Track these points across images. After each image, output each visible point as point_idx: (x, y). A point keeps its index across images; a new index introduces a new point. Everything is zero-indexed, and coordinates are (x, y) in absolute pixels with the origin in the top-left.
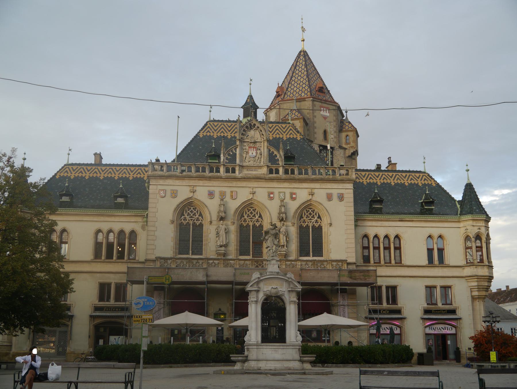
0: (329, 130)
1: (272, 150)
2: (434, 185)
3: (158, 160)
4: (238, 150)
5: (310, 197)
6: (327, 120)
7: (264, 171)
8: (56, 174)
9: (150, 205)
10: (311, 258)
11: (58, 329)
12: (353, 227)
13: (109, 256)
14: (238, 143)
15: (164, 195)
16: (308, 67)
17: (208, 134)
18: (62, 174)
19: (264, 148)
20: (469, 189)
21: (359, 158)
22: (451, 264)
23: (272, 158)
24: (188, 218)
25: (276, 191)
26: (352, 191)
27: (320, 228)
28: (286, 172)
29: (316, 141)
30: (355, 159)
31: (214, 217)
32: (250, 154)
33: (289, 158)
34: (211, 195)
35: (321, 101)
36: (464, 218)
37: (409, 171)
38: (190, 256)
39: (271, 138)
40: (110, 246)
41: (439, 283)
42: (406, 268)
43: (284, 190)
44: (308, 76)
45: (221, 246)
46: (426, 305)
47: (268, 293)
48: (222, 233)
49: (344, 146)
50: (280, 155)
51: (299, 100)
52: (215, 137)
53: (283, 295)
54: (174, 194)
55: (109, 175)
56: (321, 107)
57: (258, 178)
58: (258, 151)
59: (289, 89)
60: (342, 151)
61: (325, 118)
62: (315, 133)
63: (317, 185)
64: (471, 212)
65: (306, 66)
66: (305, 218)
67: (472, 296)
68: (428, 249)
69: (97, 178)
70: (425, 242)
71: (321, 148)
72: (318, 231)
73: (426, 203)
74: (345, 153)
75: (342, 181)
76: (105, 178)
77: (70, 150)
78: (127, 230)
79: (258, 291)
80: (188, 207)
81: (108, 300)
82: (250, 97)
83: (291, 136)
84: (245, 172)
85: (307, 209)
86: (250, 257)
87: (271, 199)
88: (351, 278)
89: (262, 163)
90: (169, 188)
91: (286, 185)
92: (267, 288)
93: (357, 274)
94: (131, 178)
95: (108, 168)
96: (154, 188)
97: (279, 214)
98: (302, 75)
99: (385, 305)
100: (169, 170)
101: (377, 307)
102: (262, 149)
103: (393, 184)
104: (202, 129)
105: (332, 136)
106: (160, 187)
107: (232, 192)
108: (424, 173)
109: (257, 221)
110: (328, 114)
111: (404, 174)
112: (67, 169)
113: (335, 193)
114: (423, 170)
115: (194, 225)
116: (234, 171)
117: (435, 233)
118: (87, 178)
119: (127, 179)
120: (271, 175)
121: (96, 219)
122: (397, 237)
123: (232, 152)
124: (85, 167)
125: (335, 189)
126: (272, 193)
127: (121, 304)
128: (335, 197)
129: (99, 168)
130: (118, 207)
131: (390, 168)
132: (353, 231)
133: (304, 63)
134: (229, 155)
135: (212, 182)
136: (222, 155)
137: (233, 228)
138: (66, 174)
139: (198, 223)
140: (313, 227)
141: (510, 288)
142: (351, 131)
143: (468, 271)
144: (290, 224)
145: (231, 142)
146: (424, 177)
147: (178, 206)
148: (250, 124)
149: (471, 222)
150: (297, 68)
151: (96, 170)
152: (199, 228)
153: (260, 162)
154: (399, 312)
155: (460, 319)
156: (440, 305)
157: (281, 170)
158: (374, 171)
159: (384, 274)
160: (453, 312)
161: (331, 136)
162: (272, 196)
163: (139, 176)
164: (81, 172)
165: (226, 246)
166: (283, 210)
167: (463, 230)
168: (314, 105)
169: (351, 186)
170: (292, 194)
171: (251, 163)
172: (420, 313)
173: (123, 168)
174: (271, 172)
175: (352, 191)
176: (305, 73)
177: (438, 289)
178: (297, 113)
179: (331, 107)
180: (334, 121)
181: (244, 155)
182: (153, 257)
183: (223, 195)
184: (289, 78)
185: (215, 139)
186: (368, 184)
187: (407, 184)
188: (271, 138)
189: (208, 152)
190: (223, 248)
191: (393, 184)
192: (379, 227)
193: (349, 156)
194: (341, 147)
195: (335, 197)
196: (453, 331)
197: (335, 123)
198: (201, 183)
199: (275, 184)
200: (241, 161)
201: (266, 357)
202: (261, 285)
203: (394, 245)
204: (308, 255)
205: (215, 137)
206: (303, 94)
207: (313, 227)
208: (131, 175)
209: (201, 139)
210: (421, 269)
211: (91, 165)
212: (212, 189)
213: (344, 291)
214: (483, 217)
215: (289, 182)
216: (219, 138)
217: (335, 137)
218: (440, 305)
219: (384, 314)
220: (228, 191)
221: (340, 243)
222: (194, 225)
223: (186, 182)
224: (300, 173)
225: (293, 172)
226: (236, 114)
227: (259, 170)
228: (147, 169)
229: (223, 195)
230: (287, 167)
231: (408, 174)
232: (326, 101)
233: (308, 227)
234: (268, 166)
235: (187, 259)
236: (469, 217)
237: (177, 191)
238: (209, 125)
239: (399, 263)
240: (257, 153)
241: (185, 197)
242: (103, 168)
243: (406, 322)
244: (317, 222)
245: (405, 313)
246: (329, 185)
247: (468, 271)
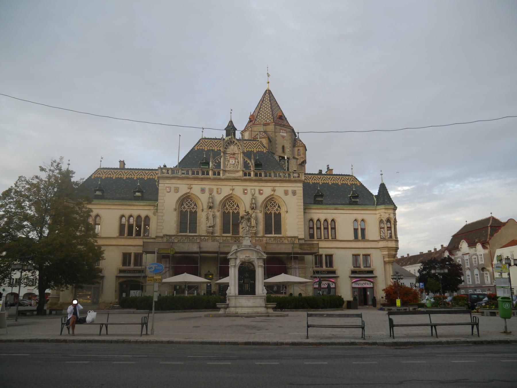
0: (286, 146)
1: (246, 159)
2: (359, 184)
3: (165, 166)
4: (222, 159)
5: (273, 193)
6: (285, 138)
7: (241, 174)
8: (92, 176)
9: (159, 198)
10: (273, 235)
11: (93, 286)
12: (303, 213)
13: (130, 233)
14: (222, 154)
15: (169, 191)
17: (201, 148)
18: (96, 176)
19: (241, 158)
20: (383, 188)
21: (306, 166)
22: (370, 239)
23: (246, 165)
25: (249, 188)
27: (280, 214)
28: (256, 175)
29: (277, 153)
30: (304, 166)
31: (205, 207)
32: (231, 162)
33: (258, 165)
34: (203, 190)
35: (280, 125)
36: (379, 207)
37: (342, 175)
38: (188, 234)
39: (245, 151)
40: (131, 227)
41: (362, 252)
42: (339, 242)
44: (271, 108)
45: (210, 227)
46: (353, 268)
47: (243, 260)
48: (211, 217)
49: (296, 157)
50: (252, 163)
51: (265, 125)
52: (206, 150)
53: (254, 261)
54: (177, 190)
55: (130, 177)
56: (280, 129)
57: (236, 179)
58: (237, 160)
59: (258, 117)
60: (295, 160)
61: (283, 137)
62: (276, 148)
63: (278, 184)
64: (384, 203)
65: (270, 101)
66: (269, 207)
67: (384, 261)
68: (354, 229)
69: (121, 179)
70: (352, 224)
72: (278, 216)
73: (353, 197)
74: (297, 162)
75: (295, 181)
76: (127, 179)
77: (102, 158)
78: (143, 216)
79: (236, 259)
80: (186, 199)
81: (129, 264)
82: (231, 122)
83: (260, 150)
84: (227, 175)
85: (271, 201)
86: (230, 235)
87: (246, 194)
88: (301, 249)
89: (239, 169)
90: (173, 186)
91: (256, 184)
92: (242, 257)
93: (305, 247)
94: (146, 179)
95: (129, 171)
96: (162, 186)
97: (251, 204)
98: (268, 107)
99: (324, 267)
100: (173, 173)
101: (319, 269)
102: (239, 158)
103: (330, 184)
104: (197, 144)
105: (288, 150)
106: (167, 185)
107: (217, 189)
108: (352, 176)
109: (236, 209)
110: (285, 134)
111: (338, 177)
112: (100, 172)
113: (290, 189)
114: (351, 174)
115: (191, 212)
116: (219, 174)
117: (359, 217)
118: (114, 178)
119: (143, 179)
120: (245, 177)
121: (120, 207)
122: (333, 220)
124: (112, 171)
125: (290, 187)
126: (246, 190)
127: (139, 268)
128: (290, 193)
129: (123, 171)
130: (137, 199)
131: (328, 173)
132: (303, 216)
134: (216, 162)
136: (211, 163)
137: (218, 214)
138: (99, 176)
139: (193, 211)
140: (275, 213)
141: (410, 255)
142: (301, 146)
143: (382, 244)
144: (258, 211)
145: (217, 154)
147: (179, 198)
148: (231, 141)
149: (383, 211)
150: (264, 102)
151: (121, 173)
152: (194, 214)
154: (334, 272)
155: (376, 277)
156: (362, 267)
157: (252, 174)
158: (317, 174)
159: (324, 246)
160: (371, 272)
161: (287, 150)
162: (246, 191)
163: (151, 177)
164: (110, 174)
165: (213, 227)
166: (254, 201)
168: (275, 128)
169: (301, 185)
170: (260, 190)
171: (232, 169)
172: (348, 273)
173: (140, 171)
174: (245, 174)
175: (302, 188)
176: (270, 105)
177: (361, 256)
178: (264, 134)
179: (288, 130)
181: (227, 163)
182: (161, 235)
183: (211, 191)
184: (258, 109)
185: (205, 151)
186: (313, 183)
188: (245, 151)
189: (201, 160)
190: (211, 228)
191: (330, 184)
192: (320, 214)
193: (300, 164)
194: (294, 158)
195: (290, 193)
196: (371, 286)
198: (196, 182)
199: (248, 184)
200: (224, 167)
201: (241, 304)
202: (238, 254)
203: (331, 226)
204: (271, 233)
205: (206, 150)
206: (268, 121)
207: (275, 213)
208: (146, 177)
210: (349, 242)
211: (117, 169)
212: (203, 186)
213: (296, 258)
214: (392, 207)
215: (258, 182)
216: (209, 151)
217: (290, 151)
218: (362, 267)
219: (324, 274)
220: (215, 188)
221: (293, 225)
222: (191, 212)
223: (185, 182)
224: (266, 176)
225: (261, 175)
226: (221, 134)
228: (157, 172)
229: (211, 191)
230: (257, 171)
231: (341, 177)
232: (284, 126)
233: (271, 213)
236: (383, 207)
237: (178, 188)
238: (201, 141)
239: (334, 239)
240: (235, 161)
241: (185, 192)
242: (126, 171)
243: (339, 279)
244: (277, 210)
245: (338, 273)
246: (286, 184)
247: (382, 244)
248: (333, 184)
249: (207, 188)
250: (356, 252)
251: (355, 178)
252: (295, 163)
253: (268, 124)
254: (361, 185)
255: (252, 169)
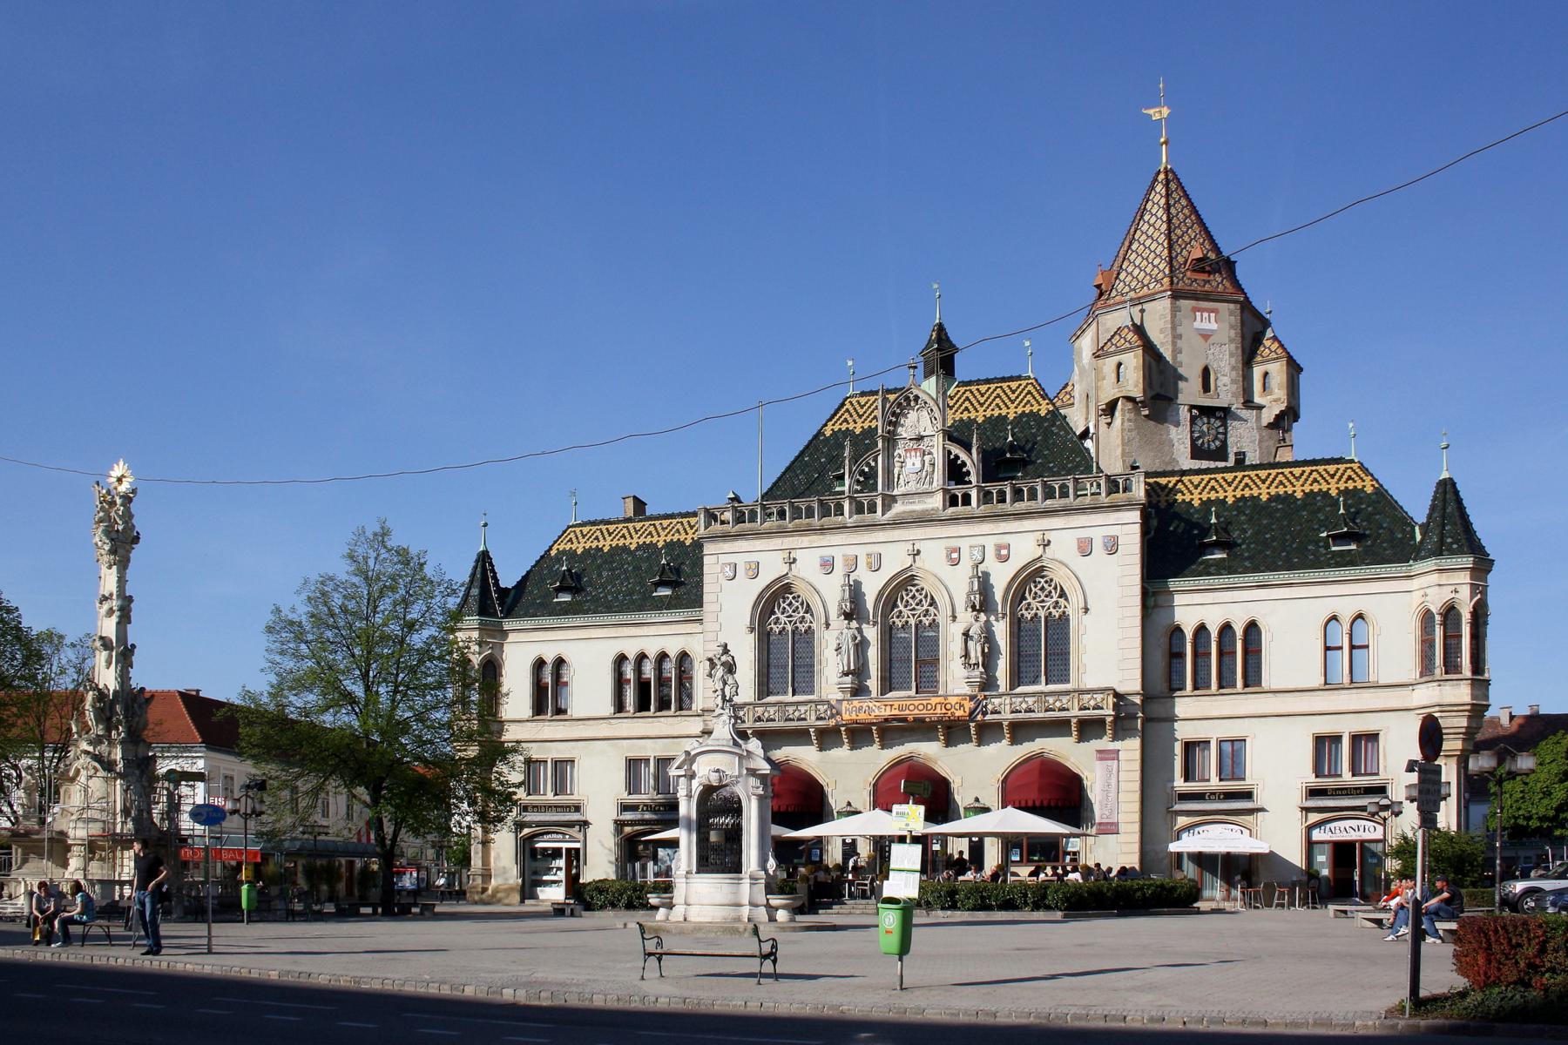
0: (1213, 366)
1: (956, 450)
2: (1369, 490)
5: (1040, 551)
6: (1211, 340)
7: (937, 501)
10: (1042, 687)
13: (643, 705)
16: (1173, 211)
17: (844, 427)
20: (1447, 493)
22: (1382, 682)
23: (955, 472)
24: (783, 618)
25: (964, 544)
26: (1137, 529)
28: (986, 497)
29: (1181, 398)
33: (998, 465)
34: (828, 565)
38: (789, 698)
40: (662, 682)
43: (981, 541)
44: (1169, 237)
50: (971, 462)
56: (1195, 310)
61: (1206, 336)
66: (1030, 600)
69: (625, 548)
70: (1320, 634)
71: (1195, 412)
78: (673, 653)
80: (777, 596)
87: (955, 563)
91: (986, 527)
96: (716, 560)
98: (1156, 235)
102: (934, 451)
103: (1264, 498)
105: (1226, 380)
107: (869, 555)
110: (1214, 326)
111: (1297, 471)
113: (1098, 535)
116: (872, 509)
119: (681, 543)
123: (868, 465)
125: (1098, 526)
128: (1098, 546)
133: (1163, 201)
134: (862, 473)
135: (828, 537)
139: (802, 628)
145: (864, 442)
146: (1349, 472)
152: (804, 640)
153: (931, 483)
155: (1262, 810)
157: (974, 494)
162: (955, 555)
167: (1416, 598)
168: (1175, 311)
169: (1135, 516)
170: (999, 548)
171: (912, 487)
172: (1297, 798)
174: (953, 501)
180: (1231, 341)
187: (1299, 495)
191: (1264, 498)
192: (1199, 606)
195: (1098, 546)
197: (1233, 346)
198: (805, 541)
204: (1035, 681)
209: (827, 439)
217: (1233, 381)
220: (861, 552)
223: (777, 542)
227: (929, 500)
228: (693, 520)
230: (989, 486)
234: (945, 491)
235: (774, 704)
238: (848, 406)
248: (1275, 498)
249: (838, 555)
250: (1326, 726)
251: (1362, 467)
252: (1252, 423)
253: (1151, 298)
254: (1381, 493)
255: (973, 478)
